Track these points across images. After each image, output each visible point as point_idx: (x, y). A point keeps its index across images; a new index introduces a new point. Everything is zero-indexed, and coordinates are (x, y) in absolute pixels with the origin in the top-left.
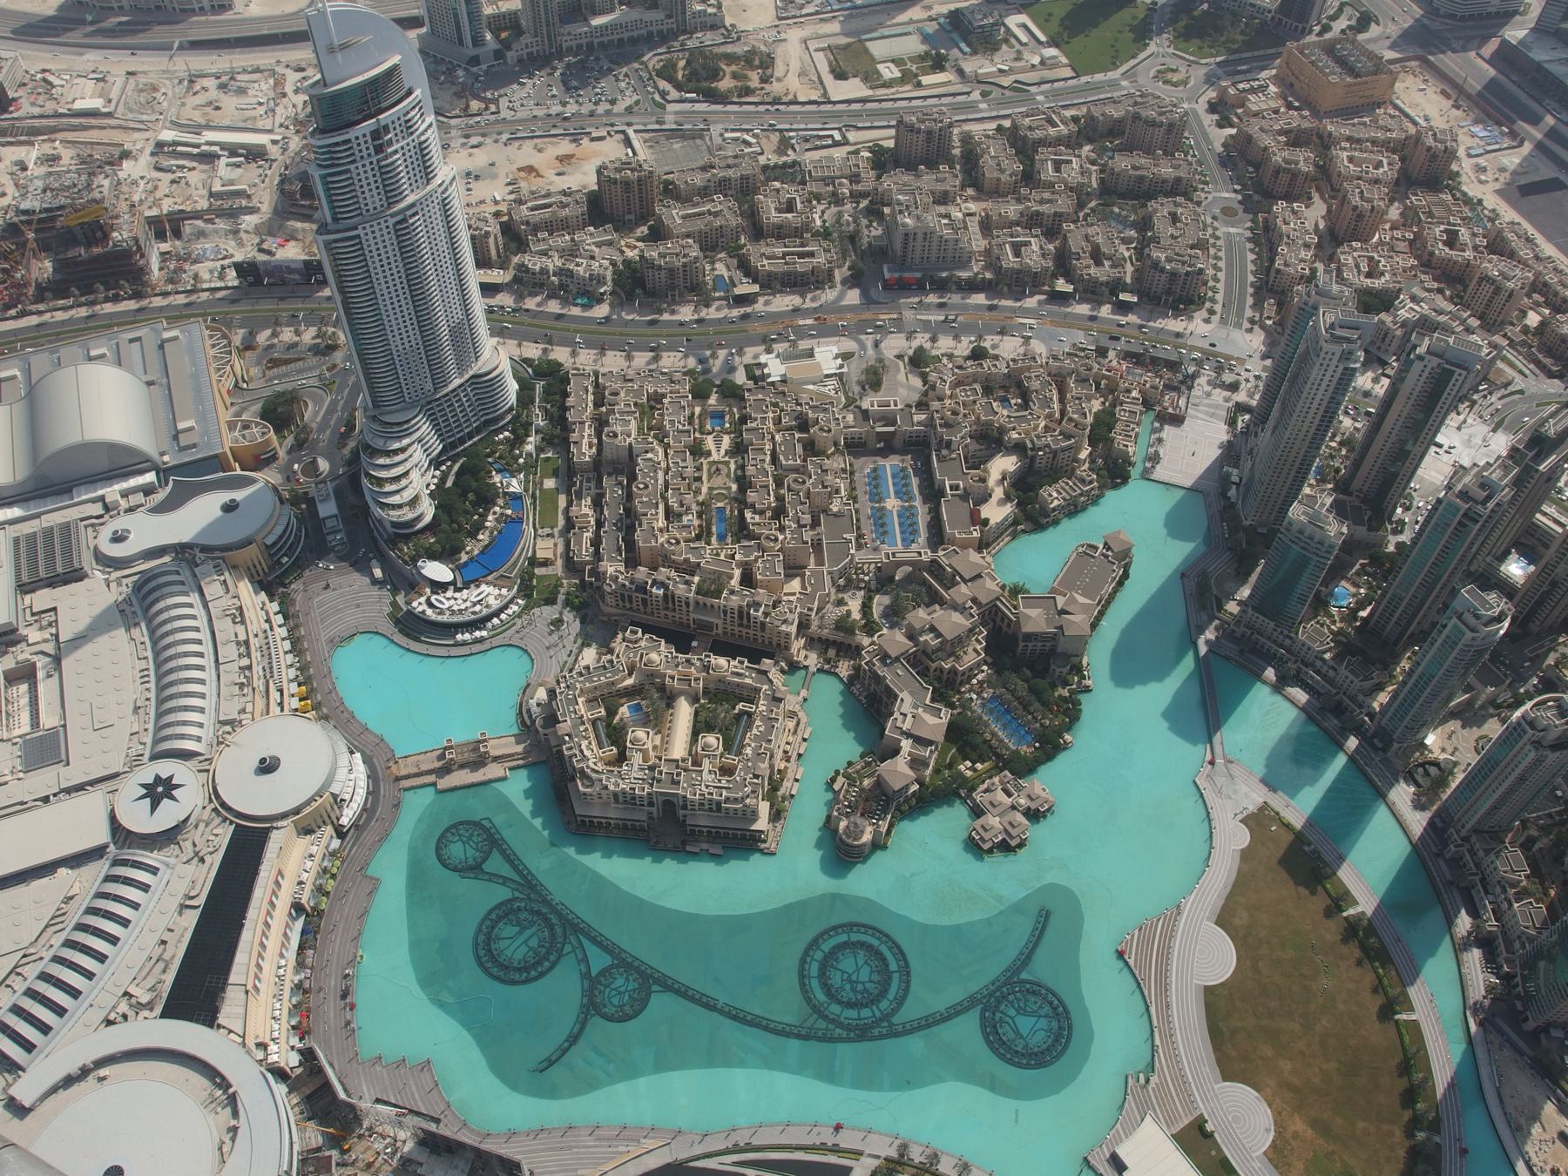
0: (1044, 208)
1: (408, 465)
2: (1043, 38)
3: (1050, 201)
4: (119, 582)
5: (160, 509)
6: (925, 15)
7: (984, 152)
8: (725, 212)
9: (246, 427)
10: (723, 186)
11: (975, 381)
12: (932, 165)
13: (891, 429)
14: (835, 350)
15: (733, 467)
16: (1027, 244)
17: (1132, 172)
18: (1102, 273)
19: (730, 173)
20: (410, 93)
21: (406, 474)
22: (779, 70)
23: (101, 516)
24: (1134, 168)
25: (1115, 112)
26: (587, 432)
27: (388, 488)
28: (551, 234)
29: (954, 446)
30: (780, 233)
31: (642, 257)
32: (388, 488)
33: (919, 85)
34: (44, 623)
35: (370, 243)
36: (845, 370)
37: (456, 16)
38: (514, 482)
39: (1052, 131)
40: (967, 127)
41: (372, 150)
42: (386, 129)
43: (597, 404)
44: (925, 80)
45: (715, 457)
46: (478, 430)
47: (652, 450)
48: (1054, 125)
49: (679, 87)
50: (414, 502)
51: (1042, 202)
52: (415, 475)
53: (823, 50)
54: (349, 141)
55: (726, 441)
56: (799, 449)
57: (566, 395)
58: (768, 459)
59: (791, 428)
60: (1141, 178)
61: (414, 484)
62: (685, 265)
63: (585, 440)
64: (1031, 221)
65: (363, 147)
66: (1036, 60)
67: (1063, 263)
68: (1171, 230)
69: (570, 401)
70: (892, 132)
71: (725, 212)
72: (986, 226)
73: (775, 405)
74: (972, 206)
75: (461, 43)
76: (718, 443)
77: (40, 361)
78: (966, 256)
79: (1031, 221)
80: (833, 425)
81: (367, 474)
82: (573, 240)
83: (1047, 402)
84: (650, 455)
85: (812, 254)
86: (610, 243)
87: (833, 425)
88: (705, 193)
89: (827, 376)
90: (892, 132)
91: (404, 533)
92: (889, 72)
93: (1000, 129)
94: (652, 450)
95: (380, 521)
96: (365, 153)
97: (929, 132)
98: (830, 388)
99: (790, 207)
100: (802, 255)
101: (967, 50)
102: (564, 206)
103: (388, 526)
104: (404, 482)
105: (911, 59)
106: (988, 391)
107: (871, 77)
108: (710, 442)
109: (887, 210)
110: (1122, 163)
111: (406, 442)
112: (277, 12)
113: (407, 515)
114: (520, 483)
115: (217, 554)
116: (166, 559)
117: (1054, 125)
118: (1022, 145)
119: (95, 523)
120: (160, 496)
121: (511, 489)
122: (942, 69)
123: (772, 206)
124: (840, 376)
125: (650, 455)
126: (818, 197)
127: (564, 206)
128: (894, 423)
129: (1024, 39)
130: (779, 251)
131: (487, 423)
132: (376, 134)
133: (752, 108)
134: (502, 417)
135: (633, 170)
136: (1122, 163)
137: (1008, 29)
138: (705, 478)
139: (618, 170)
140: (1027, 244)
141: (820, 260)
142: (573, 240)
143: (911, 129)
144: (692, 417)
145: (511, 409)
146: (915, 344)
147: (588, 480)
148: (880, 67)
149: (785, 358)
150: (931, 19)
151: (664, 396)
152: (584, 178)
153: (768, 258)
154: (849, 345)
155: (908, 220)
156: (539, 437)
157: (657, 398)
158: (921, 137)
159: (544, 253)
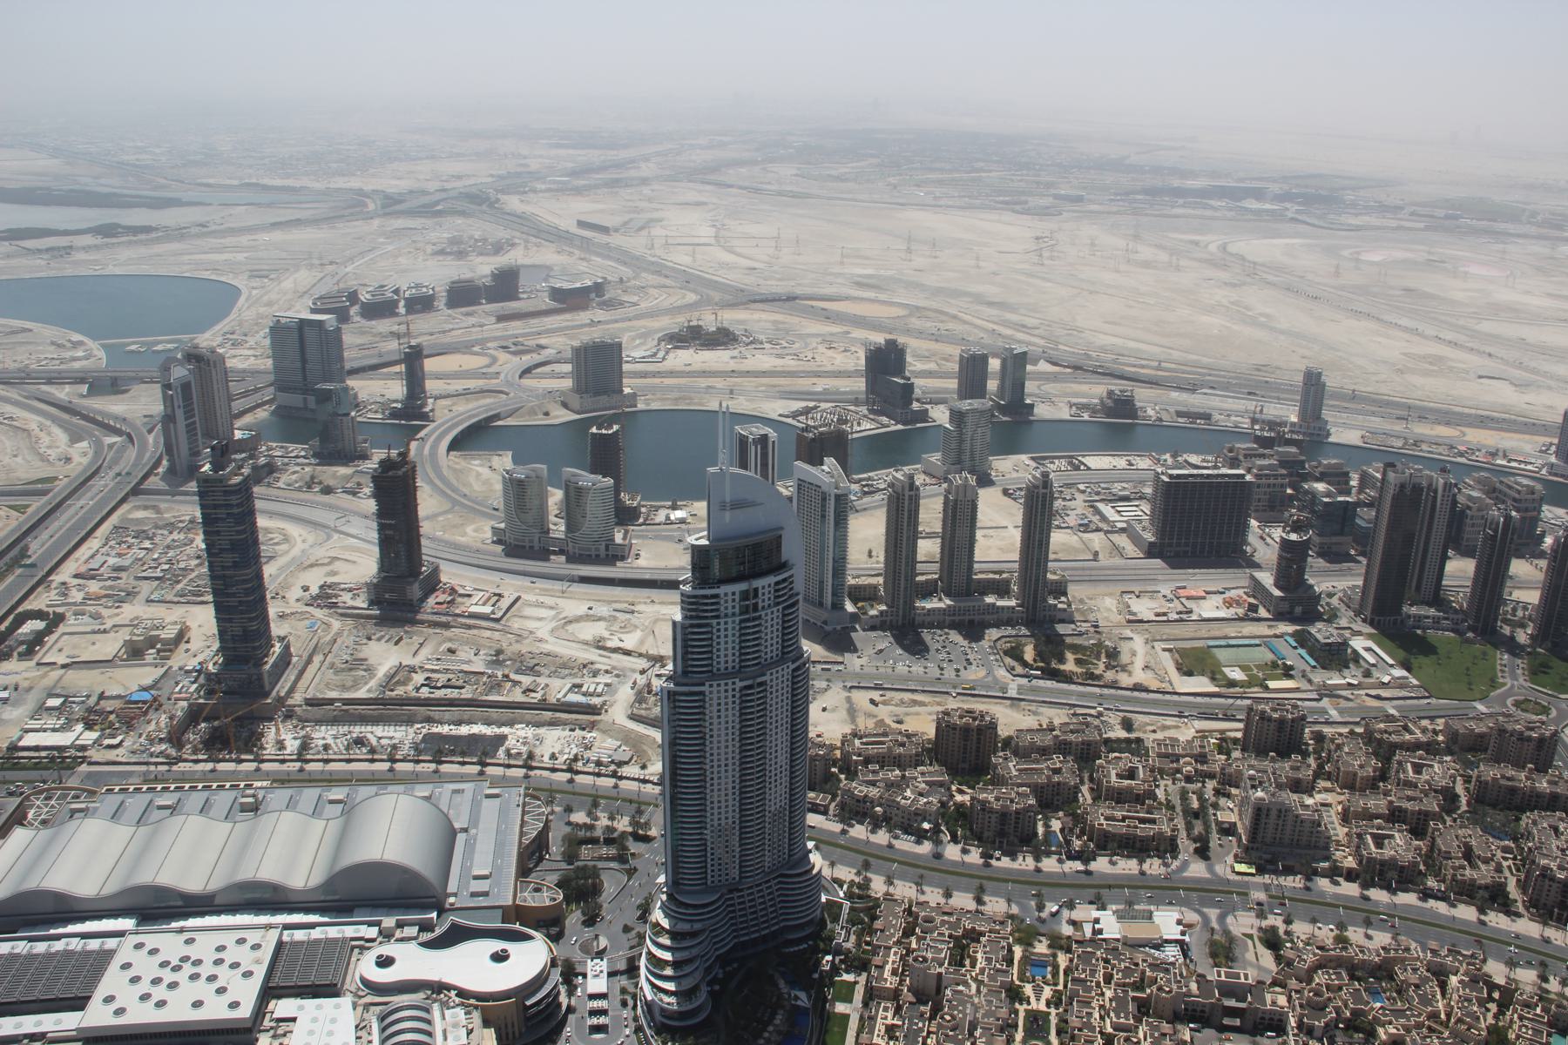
0: (1408, 805)
1: (695, 951)
2: (1391, 661)
3: (1414, 799)
4: (367, 1006)
5: (428, 945)
6: (1270, 632)
7: (1339, 747)
8: (1062, 768)
9: (537, 890)
10: (1063, 747)
11: (1340, 966)
12: (1283, 754)
13: (1243, 1005)
14: (1176, 916)
15: (1054, 1020)
16: (1391, 837)
17: (1503, 782)
18: (1482, 874)
19: (1072, 737)
20: (783, 566)
22: (1124, 658)
23: (373, 940)
24: (1503, 777)
25: (1480, 728)
26: (892, 958)
28: (882, 767)
29: (1318, 1033)
30: (1119, 797)
31: (973, 799)
33: (1267, 688)
34: (280, 1031)
35: (711, 710)
36: (1187, 938)
37: (822, 582)
38: (802, 995)
39: (1408, 737)
40: (1317, 728)
41: (737, 610)
42: (756, 590)
43: (908, 932)
44: (1272, 684)
45: (1034, 1005)
47: (966, 984)
48: (1411, 733)
49: (1025, 664)
51: (1410, 799)
53: (1169, 650)
54: (716, 596)
55: (1047, 992)
56: (1131, 1007)
57: (874, 918)
58: (1097, 1015)
59: (1124, 985)
60: (1513, 790)
62: (1017, 812)
63: (888, 967)
64: (1395, 816)
65: (730, 604)
66: (1386, 679)
67: (1433, 859)
68: (1554, 843)
69: (878, 924)
70: (1241, 725)
71: (1062, 768)
72: (1345, 817)
73: (1106, 961)
74: (1329, 798)
75: (821, 604)
76: (1038, 992)
77: (365, 791)
78: (1321, 844)
79: (1395, 816)
80: (1174, 987)
82: (903, 776)
83: (1426, 1000)
84: (961, 988)
85: (1153, 821)
86: (941, 784)
87: (1174, 987)
88: (1044, 752)
89: (1167, 941)
90: (1241, 725)
92: (1236, 674)
93: (1352, 732)
94: (966, 984)
96: (730, 611)
97: (1282, 721)
98: (1171, 953)
99: (1131, 774)
100: (1142, 821)
101: (1313, 663)
102: (903, 745)
105: (1258, 667)
106: (1352, 977)
107: (1215, 675)
108: (1028, 989)
109: (1234, 791)
110: (1490, 772)
112: (662, 564)
114: (809, 998)
115: (472, 1001)
116: (421, 995)
117: (1411, 733)
118: (1384, 750)
119: (364, 945)
120: (438, 931)
122: (1291, 677)
123: (1113, 773)
124: (1181, 943)
125: (961, 988)
126: (1161, 772)
127: (903, 745)
128: (1244, 1000)
129: (1372, 661)
130: (1119, 814)
132: (745, 595)
133: (1097, 690)
135: (975, 719)
136: (1490, 772)
137: (1355, 651)
138: (1021, 1023)
139: (961, 717)
140: (1391, 837)
141: (1166, 828)
142: (903, 776)
143: (1263, 716)
144: (1010, 962)
146: (1265, 924)
147: (886, 1009)
148: (1226, 670)
149: (1120, 916)
150: (1276, 636)
151: (982, 934)
152: (923, 725)
153: (1107, 819)
154: (1192, 917)
155: (1260, 794)
157: (974, 936)
158: (1272, 725)
159: (873, 784)
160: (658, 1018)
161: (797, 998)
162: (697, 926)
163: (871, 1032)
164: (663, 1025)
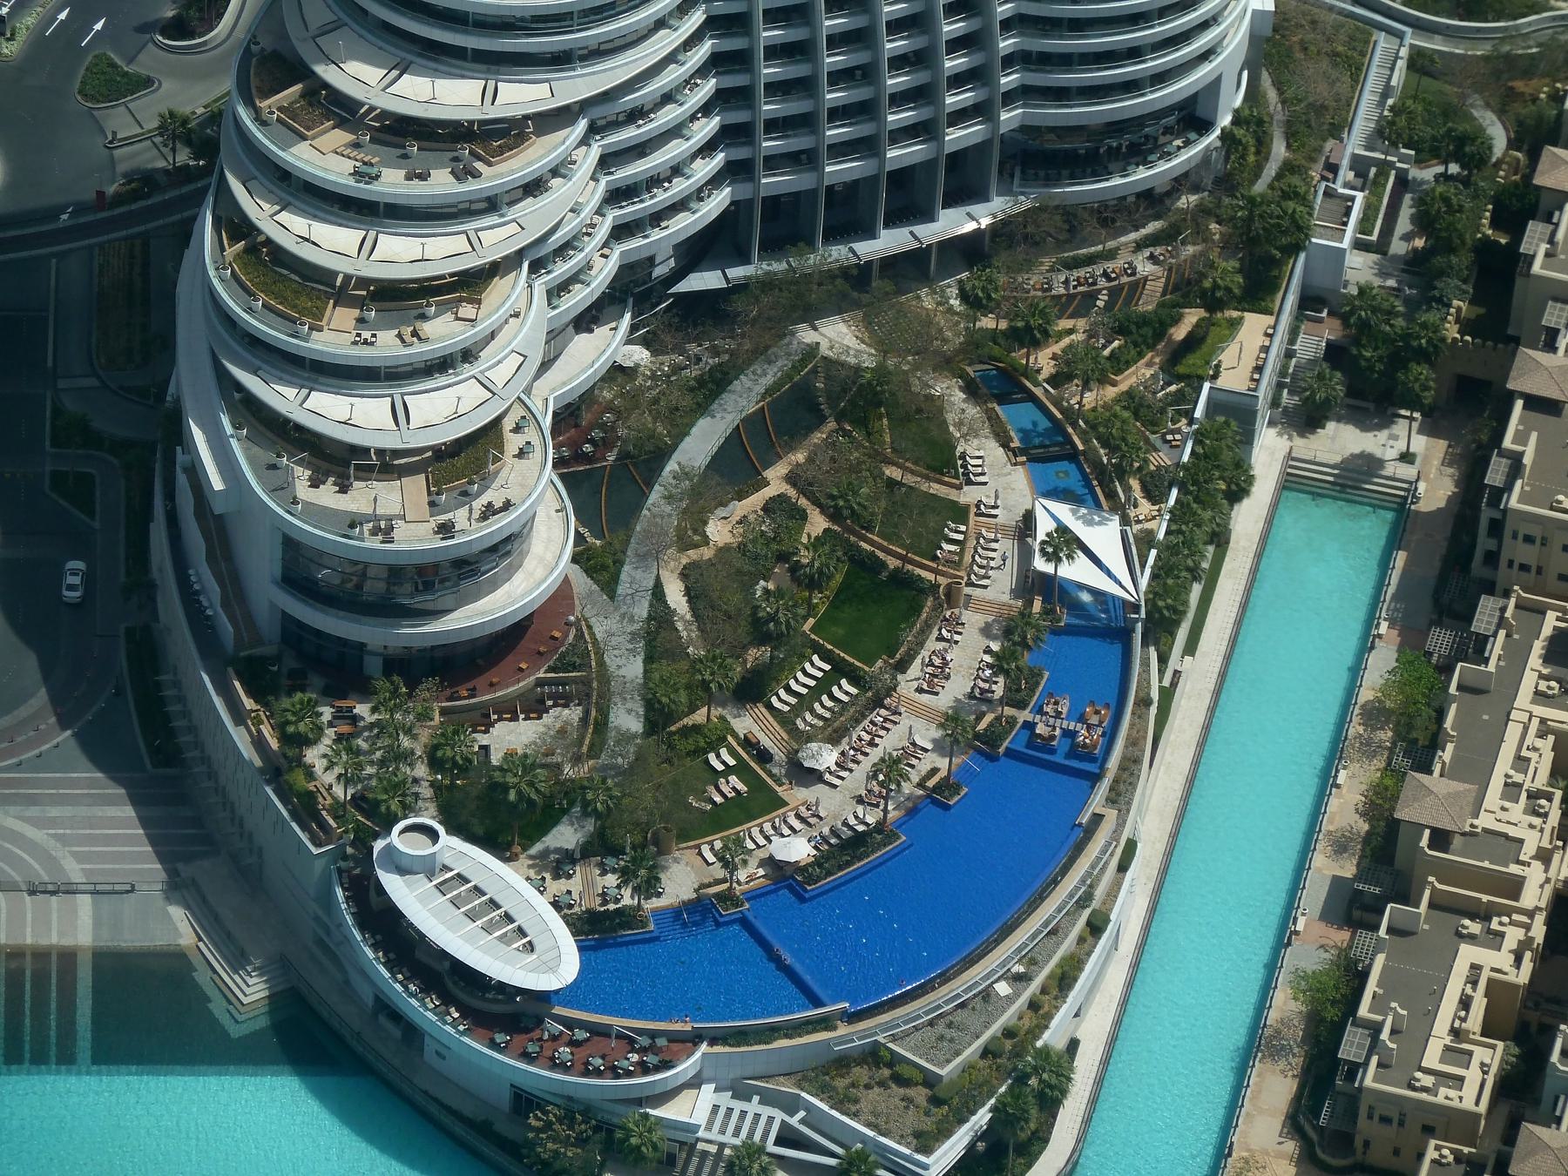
1: (496, 237)
21: (469, 284)
27: (334, 337)
32: (334, 337)
46: (963, 184)
50: (463, 460)
52: (518, 312)
61: (500, 365)
81: (237, 226)
91: (348, 636)
95: (218, 529)
103: (261, 567)
104: (442, 331)
111: (520, 95)
113: (406, 519)
114: (1137, 546)
121: (1075, 570)
131: (1033, 157)
134: (1134, 141)
145: (1191, 117)
156: (1311, 345)
160: (269, 597)
161: (1065, 543)
162: (520, 95)
163: (1475, 769)
164: (294, 632)
